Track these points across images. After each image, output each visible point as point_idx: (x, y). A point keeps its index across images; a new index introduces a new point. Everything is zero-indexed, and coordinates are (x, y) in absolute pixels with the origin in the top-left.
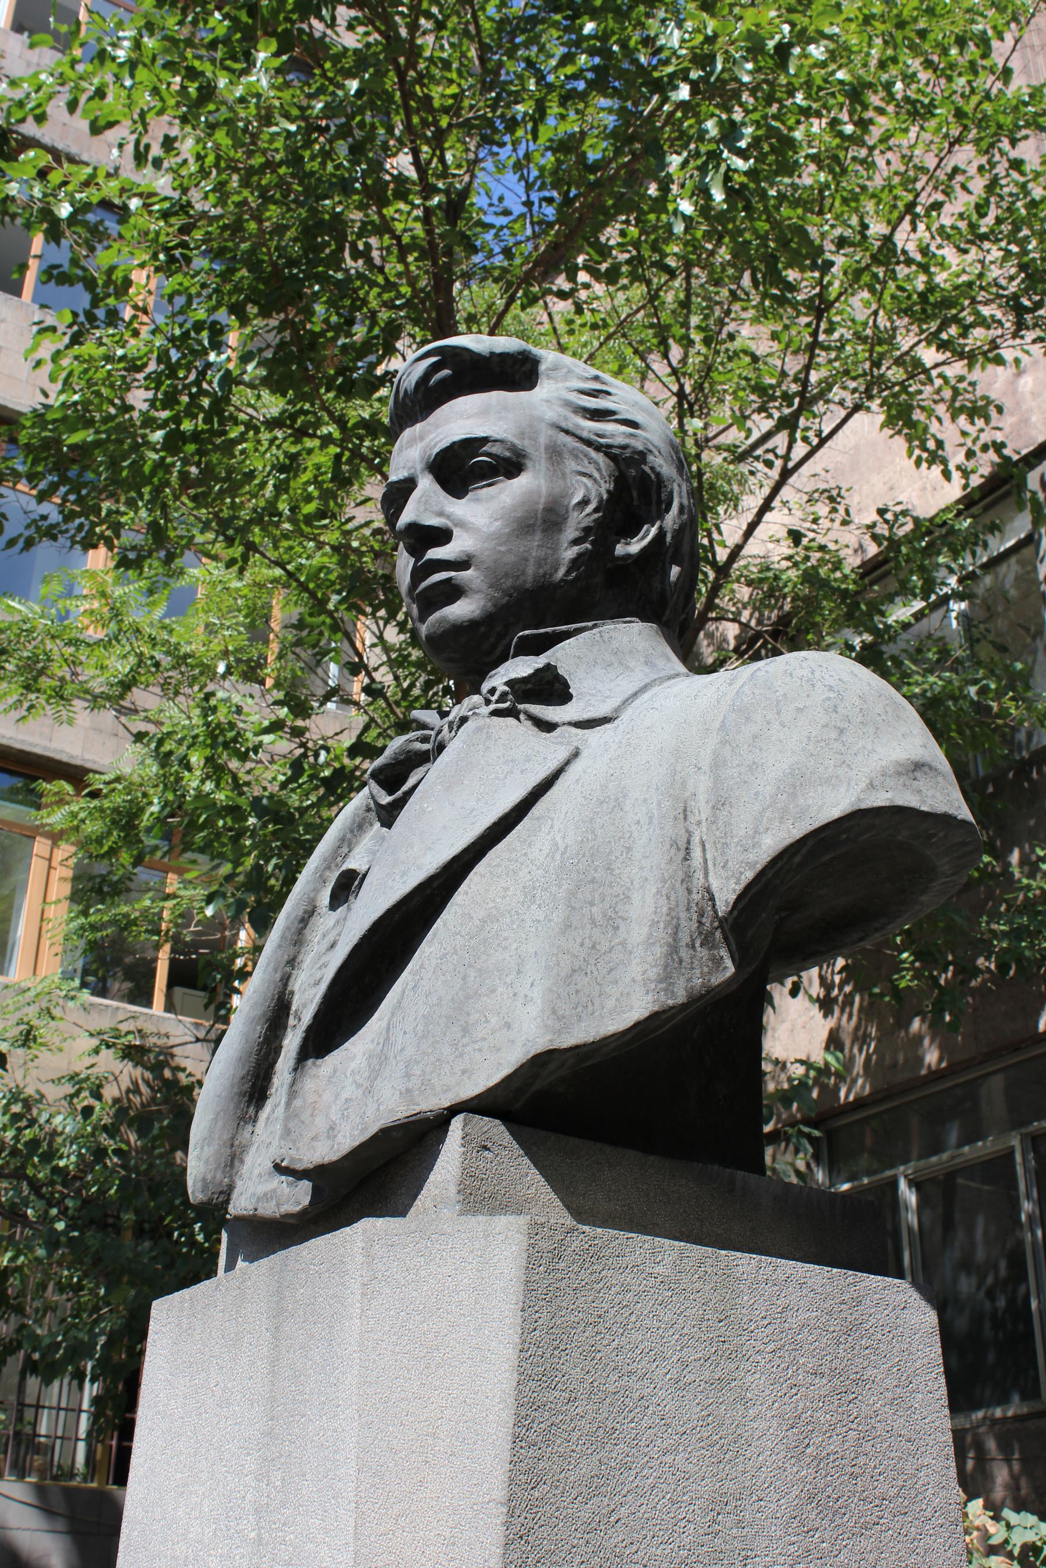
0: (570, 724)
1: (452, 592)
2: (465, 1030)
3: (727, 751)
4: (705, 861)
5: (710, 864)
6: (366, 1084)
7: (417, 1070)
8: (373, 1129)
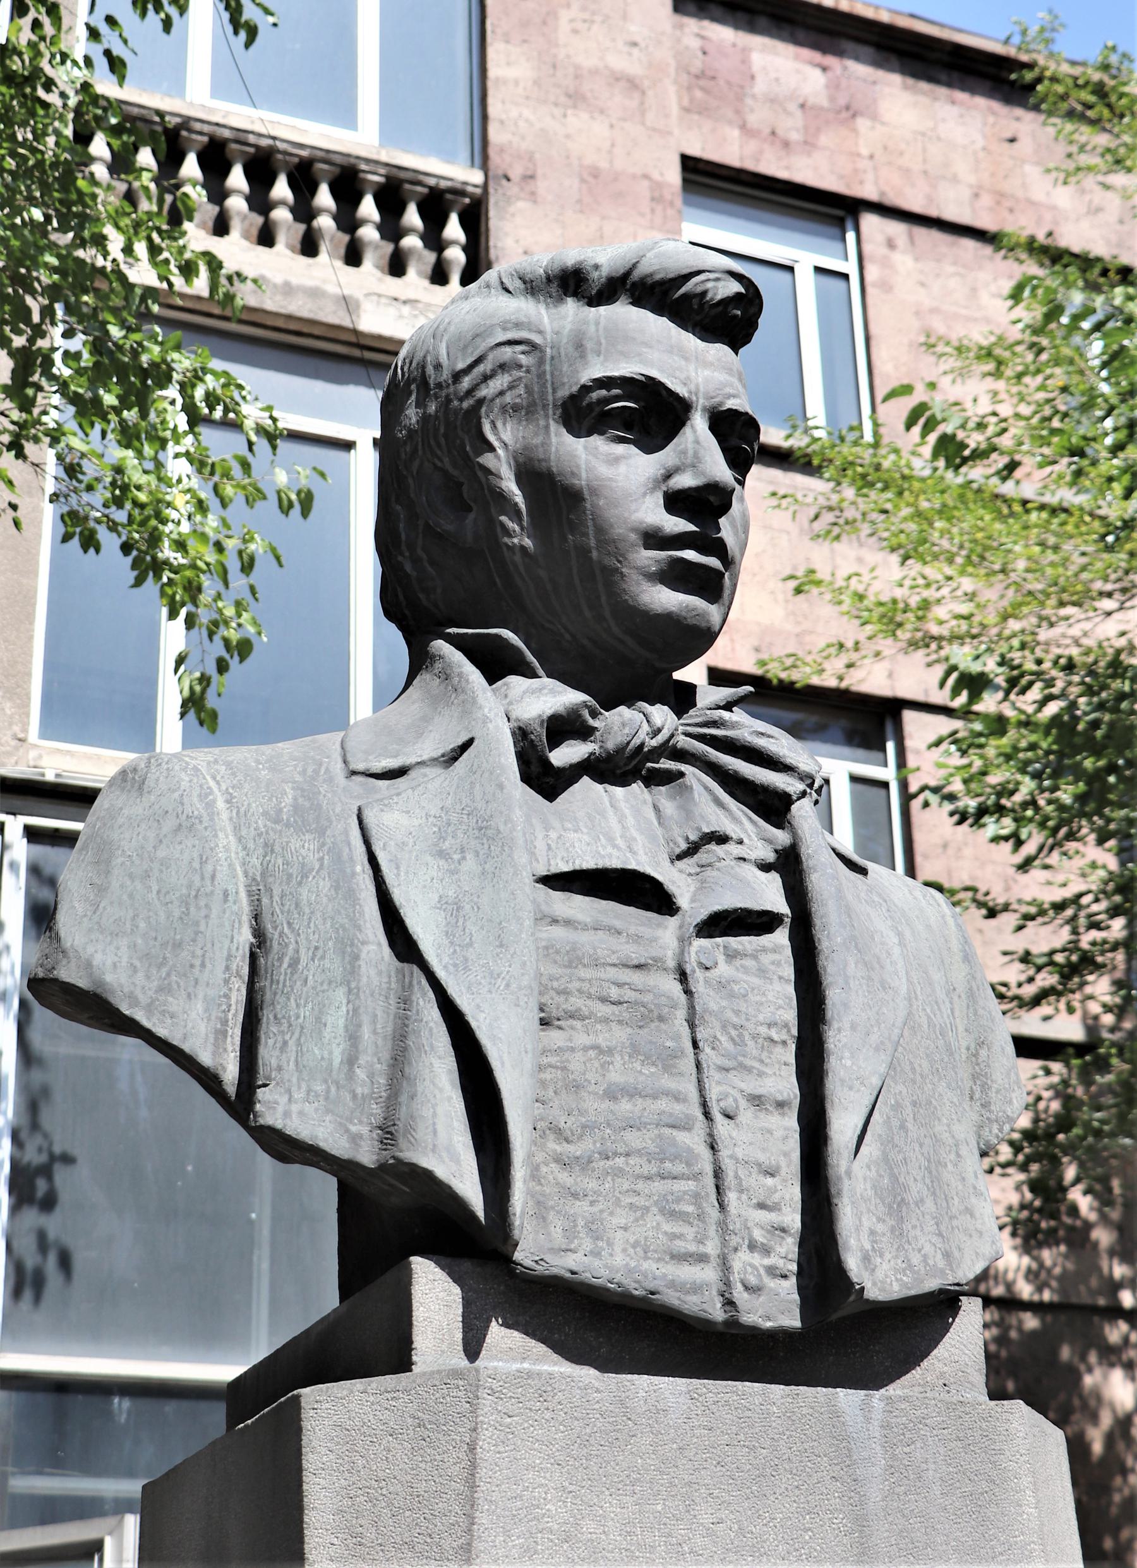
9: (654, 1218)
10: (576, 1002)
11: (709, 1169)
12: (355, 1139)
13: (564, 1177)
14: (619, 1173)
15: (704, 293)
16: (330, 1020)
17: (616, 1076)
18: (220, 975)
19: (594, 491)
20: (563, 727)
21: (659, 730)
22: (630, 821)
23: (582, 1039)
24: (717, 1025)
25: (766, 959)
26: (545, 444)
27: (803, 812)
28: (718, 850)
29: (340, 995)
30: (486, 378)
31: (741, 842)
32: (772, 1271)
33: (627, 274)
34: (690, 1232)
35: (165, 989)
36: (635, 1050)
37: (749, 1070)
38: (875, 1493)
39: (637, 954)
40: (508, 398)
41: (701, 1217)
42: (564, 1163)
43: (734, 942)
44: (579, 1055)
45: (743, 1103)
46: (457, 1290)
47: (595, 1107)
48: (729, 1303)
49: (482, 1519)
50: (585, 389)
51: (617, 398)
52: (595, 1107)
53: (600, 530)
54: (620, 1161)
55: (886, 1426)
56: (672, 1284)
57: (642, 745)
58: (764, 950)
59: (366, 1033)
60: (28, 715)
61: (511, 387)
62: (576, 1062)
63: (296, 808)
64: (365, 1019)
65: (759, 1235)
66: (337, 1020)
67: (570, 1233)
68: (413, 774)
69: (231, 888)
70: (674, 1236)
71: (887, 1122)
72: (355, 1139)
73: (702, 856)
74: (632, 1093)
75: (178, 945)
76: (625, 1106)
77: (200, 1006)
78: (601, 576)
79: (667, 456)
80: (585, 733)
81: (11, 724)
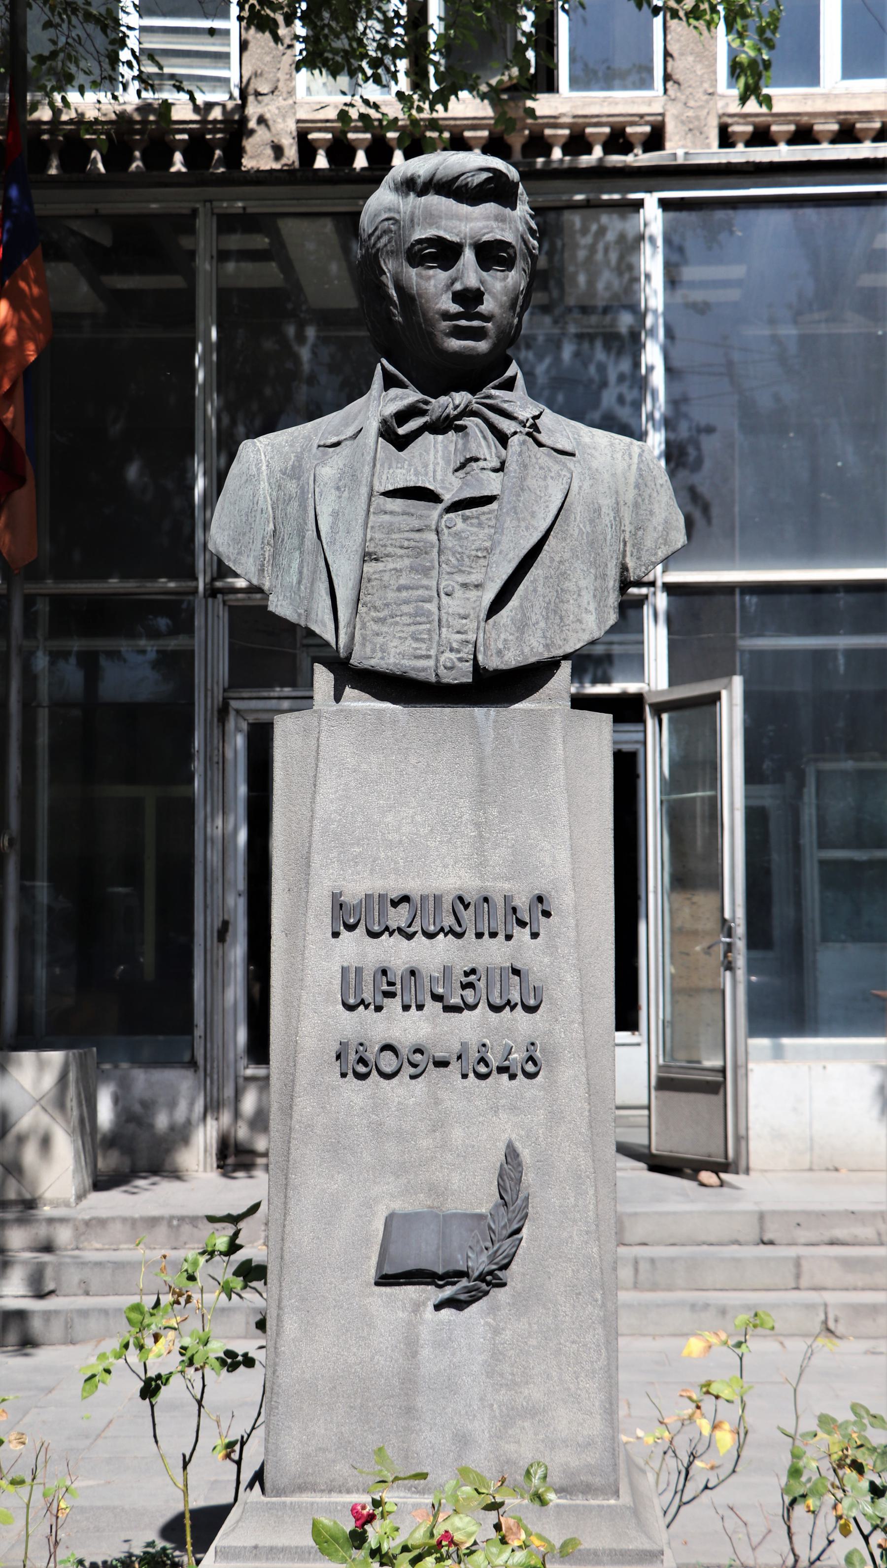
0: (553, 449)
1: (478, 334)
2: (561, 618)
3: (640, 500)
4: (625, 551)
5: (628, 554)
6: (517, 635)
7: (548, 635)
8: (533, 660)
9: (409, 642)
10: (390, 549)
11: (436, 619)
12: (299, 615)
13: (375, 627)
14: (397, 623)
15: (467, 184)
16: (293, 565)
17: (402, 581)
18: (259, 546)
19: (420, 296)
20: (403, 416)
21: (458, 406)
22: (440, 454)
23: (391, 566)
24: (450, 553)
25: (483, 518)
26: (402, 272)
27: (514, 441)
28: (473, 464)
29: (297, 554)
30: (379, 238)
31: (485, 460)
32: (461, 660)
33: (432, 179)
34: (424, 646)
35: (239, 553)
36: (412, 569)
37: (463, 572)
38: (488, 749)
39: (416, 523)
40: (389, 248)
41: (430, 639)
42: (377, 621)
43: (467, 512)
44: (388, 574)
45: (457, 587)
46: (332, 675)
47: (391, 595)
48: (437, 675)
49: (321, 765)
50: (413, 245)
51: (426, 248)
52: (391, 595)
53: (424, 315)
54: (398, 619)
55: (496, 721)
56: (413, 669)
57: (448, 415)
58: (484, 513)
59: (305, 570)
60: (715, 72)
61: (389, 242)
62: (386, 577)
63: (293, 466)
64: (305, 564)
65: (455, 645)
66: (295, 565)
67: (373, 651)
68: (343, 444)
69: (264, 507)
70: (417, 649)
71: (526, 589)
72: (299, 615)
73: (467, 469)
74: (407, 588)
75: (244, 534)
76: (404, 594)
77: (251, 560)
78: (428, 337)
79: (452, 272)
80: (423, 413)
81: (702, 82)
